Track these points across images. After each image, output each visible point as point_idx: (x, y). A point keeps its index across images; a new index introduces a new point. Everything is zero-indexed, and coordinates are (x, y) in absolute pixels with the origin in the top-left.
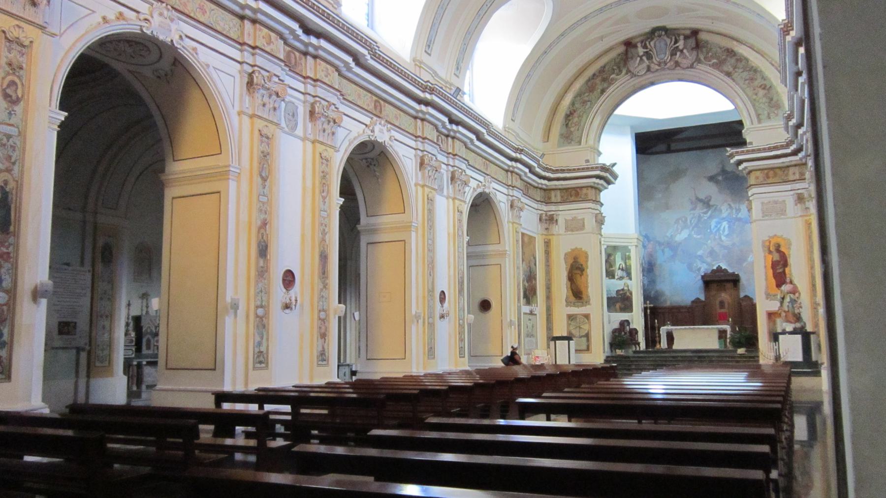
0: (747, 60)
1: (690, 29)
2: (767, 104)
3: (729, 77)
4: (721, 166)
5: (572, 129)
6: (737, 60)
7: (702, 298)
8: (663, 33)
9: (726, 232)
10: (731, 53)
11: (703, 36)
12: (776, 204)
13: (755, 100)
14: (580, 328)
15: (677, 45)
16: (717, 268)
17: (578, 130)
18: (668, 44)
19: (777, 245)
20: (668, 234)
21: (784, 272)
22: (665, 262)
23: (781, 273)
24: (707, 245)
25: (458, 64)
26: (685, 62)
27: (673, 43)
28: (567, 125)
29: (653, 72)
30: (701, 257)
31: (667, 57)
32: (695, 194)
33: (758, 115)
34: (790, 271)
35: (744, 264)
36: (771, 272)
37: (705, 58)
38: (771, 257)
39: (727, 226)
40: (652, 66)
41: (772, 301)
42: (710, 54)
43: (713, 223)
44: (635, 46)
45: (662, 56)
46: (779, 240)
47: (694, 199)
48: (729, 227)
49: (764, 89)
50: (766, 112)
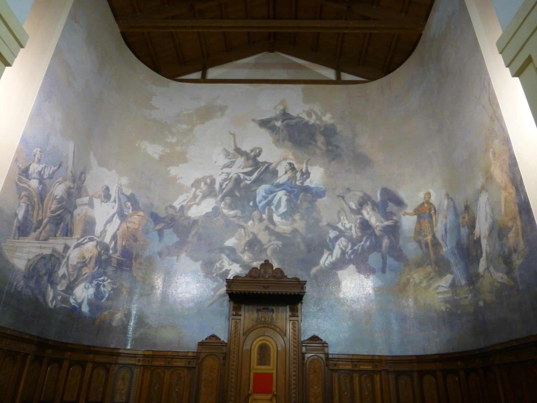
4: (281, 107)
7: (224, 337)
9: (283, 209)
16: (262, 266)
20: (177, 204)
22: (160, 254)
24: (244, 228)
30: (232, 251)
32: (235, 142)
35: (314, 270)
39: (284, 198)
43: (261, 190)
47: (231, 151)
48: (288, 201)
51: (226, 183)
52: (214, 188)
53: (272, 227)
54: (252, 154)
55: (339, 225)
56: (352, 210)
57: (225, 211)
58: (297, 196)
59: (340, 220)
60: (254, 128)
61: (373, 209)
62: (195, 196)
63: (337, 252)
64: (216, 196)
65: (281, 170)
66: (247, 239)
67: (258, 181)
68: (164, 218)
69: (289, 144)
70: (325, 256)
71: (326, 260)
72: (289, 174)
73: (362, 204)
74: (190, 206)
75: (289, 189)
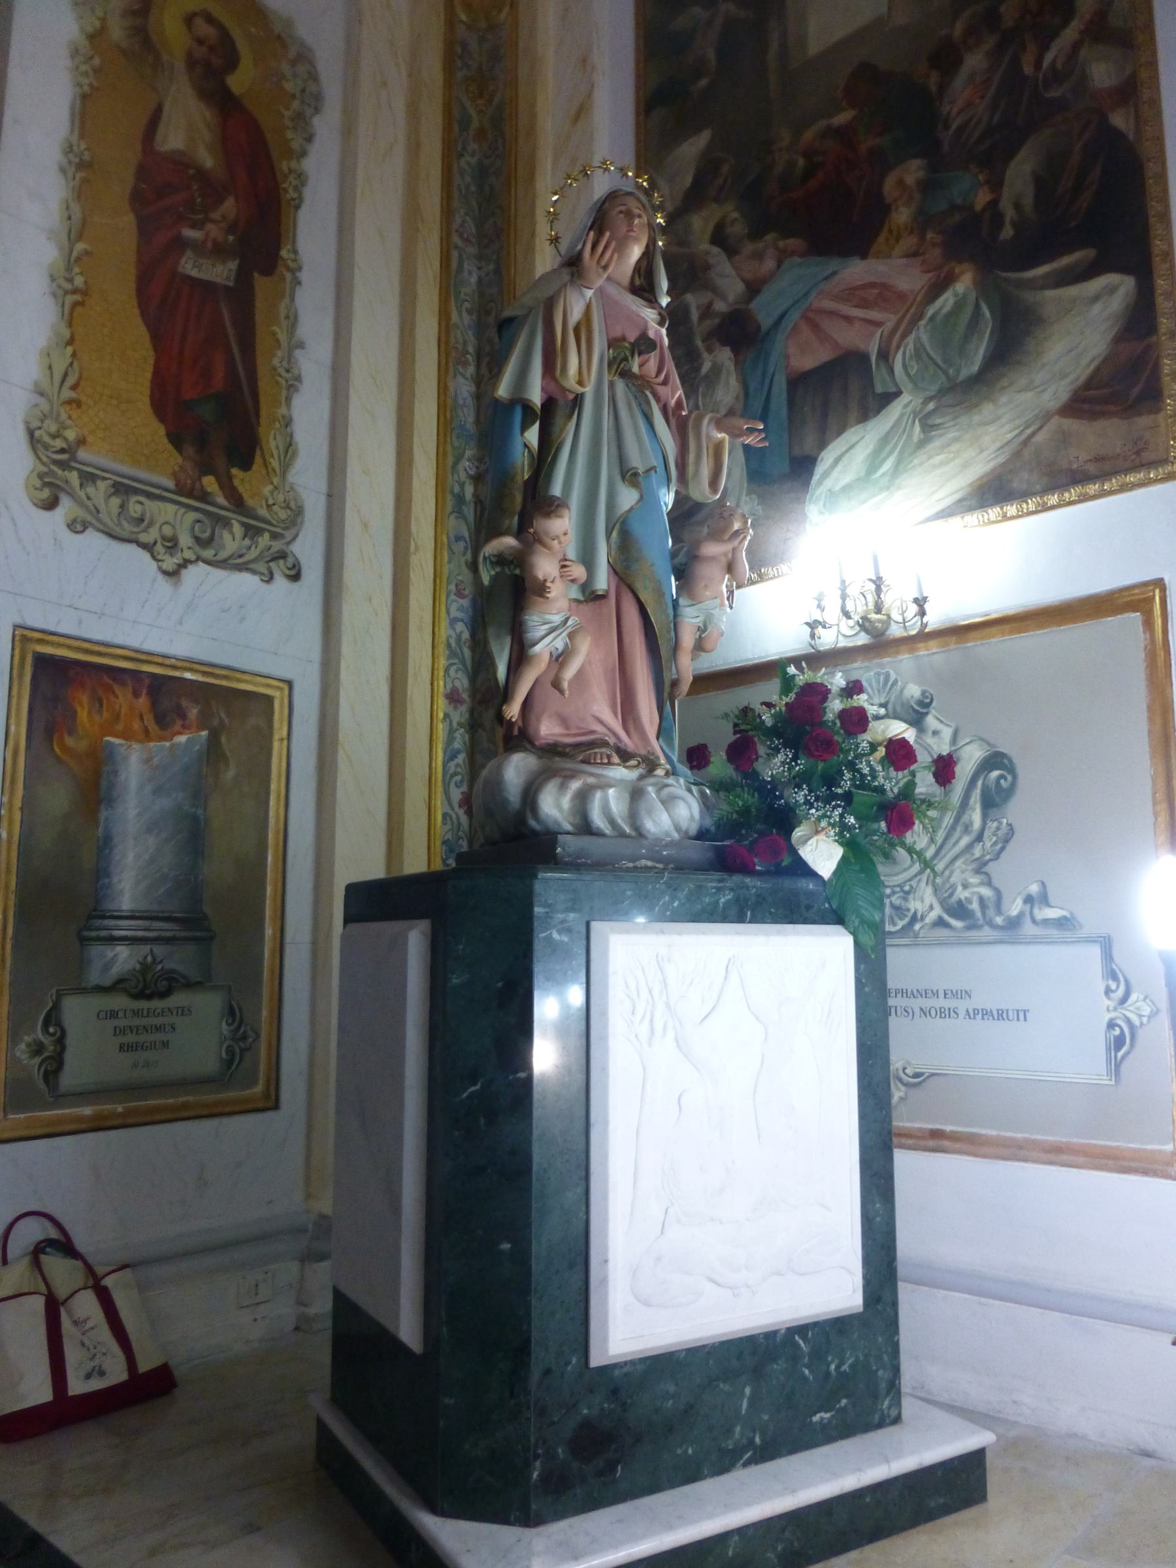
23: (208, 287)
41: (94, 541)
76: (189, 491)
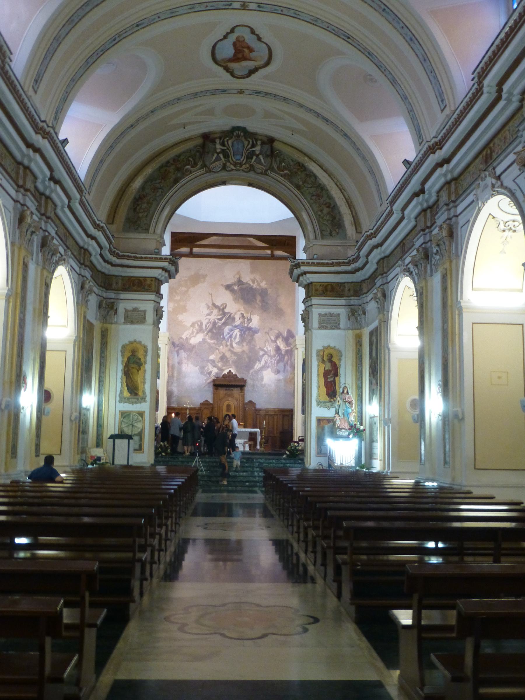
0: (316, 177)
1: (266, 136)
2: (329, 222)
3: (298, 190)
4: (237, 276)
5: (141, 215)
6: (307, 175)
7: (211, 401)
8: (242, 134)
9: (238, 340)
10: (302, 167)
11: (276, 145)
12: (332, 316)
13: (320, 216)
14: (133, 426)
15: (253, 149)
16: (228, 373)
17: (146, 216)
18: (246, 146)
19: (329, 355)
20: (184, 337)
21: (334, 381)
23: (331, 381)
25: (57, 113)
26: (259, 168)
27: (250, 146)
28: (135, 210)
29: (228, 171)
30: (213, 362)
31: (243, 159)
32: (212, 300)
33: (322, 231)
34: (340, 381)
35: (251, 371)
36: (322, 380)
37: (278, 168)
38: (323, 366)
39: (238, 334)
40: (228, 164)
42: (283, 164)
43: (227, 329)
44: (213, 141)
45: (238, 157)
46: (332, 351)
47: (210, 305)
49: (328, 207)
50: (328, 230)
51: (208, 325)
52: (202, 328)
53: (232, 349)
54: (222, 307)
55: (265, 349)
56: (272, 341)
57: (209, 341)
58: (245, 333)
59: (265, 346)
60: (222, 290)
61: (282, 340)
62: (193, 332)
63: (263, 362)
64: (203, 332)
65: (237, 317)
66: (220, 355)
67: (225, 324)
68: (178, 344)
69: (241, 301)
70: (257, 364)
71: (257, 366)
72: (241, 320)
73: (277, 337)
74: (190, 338)
75: (241, 329)
76: (330, 401)
